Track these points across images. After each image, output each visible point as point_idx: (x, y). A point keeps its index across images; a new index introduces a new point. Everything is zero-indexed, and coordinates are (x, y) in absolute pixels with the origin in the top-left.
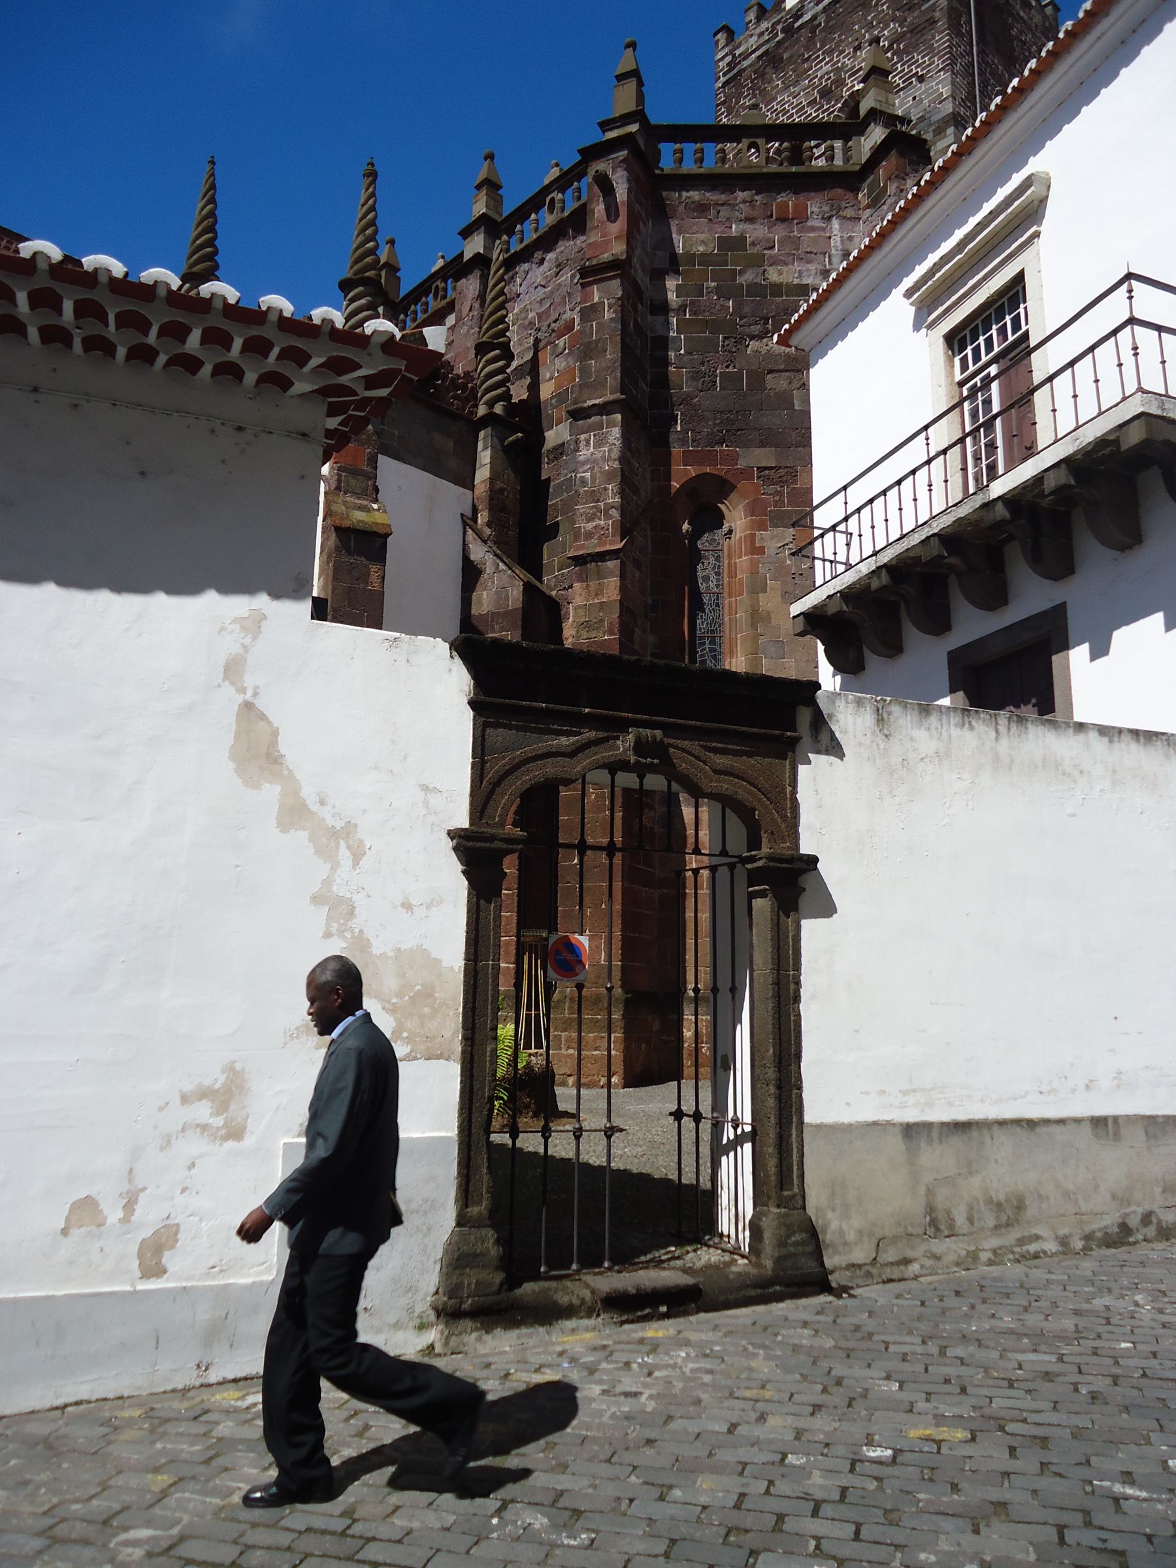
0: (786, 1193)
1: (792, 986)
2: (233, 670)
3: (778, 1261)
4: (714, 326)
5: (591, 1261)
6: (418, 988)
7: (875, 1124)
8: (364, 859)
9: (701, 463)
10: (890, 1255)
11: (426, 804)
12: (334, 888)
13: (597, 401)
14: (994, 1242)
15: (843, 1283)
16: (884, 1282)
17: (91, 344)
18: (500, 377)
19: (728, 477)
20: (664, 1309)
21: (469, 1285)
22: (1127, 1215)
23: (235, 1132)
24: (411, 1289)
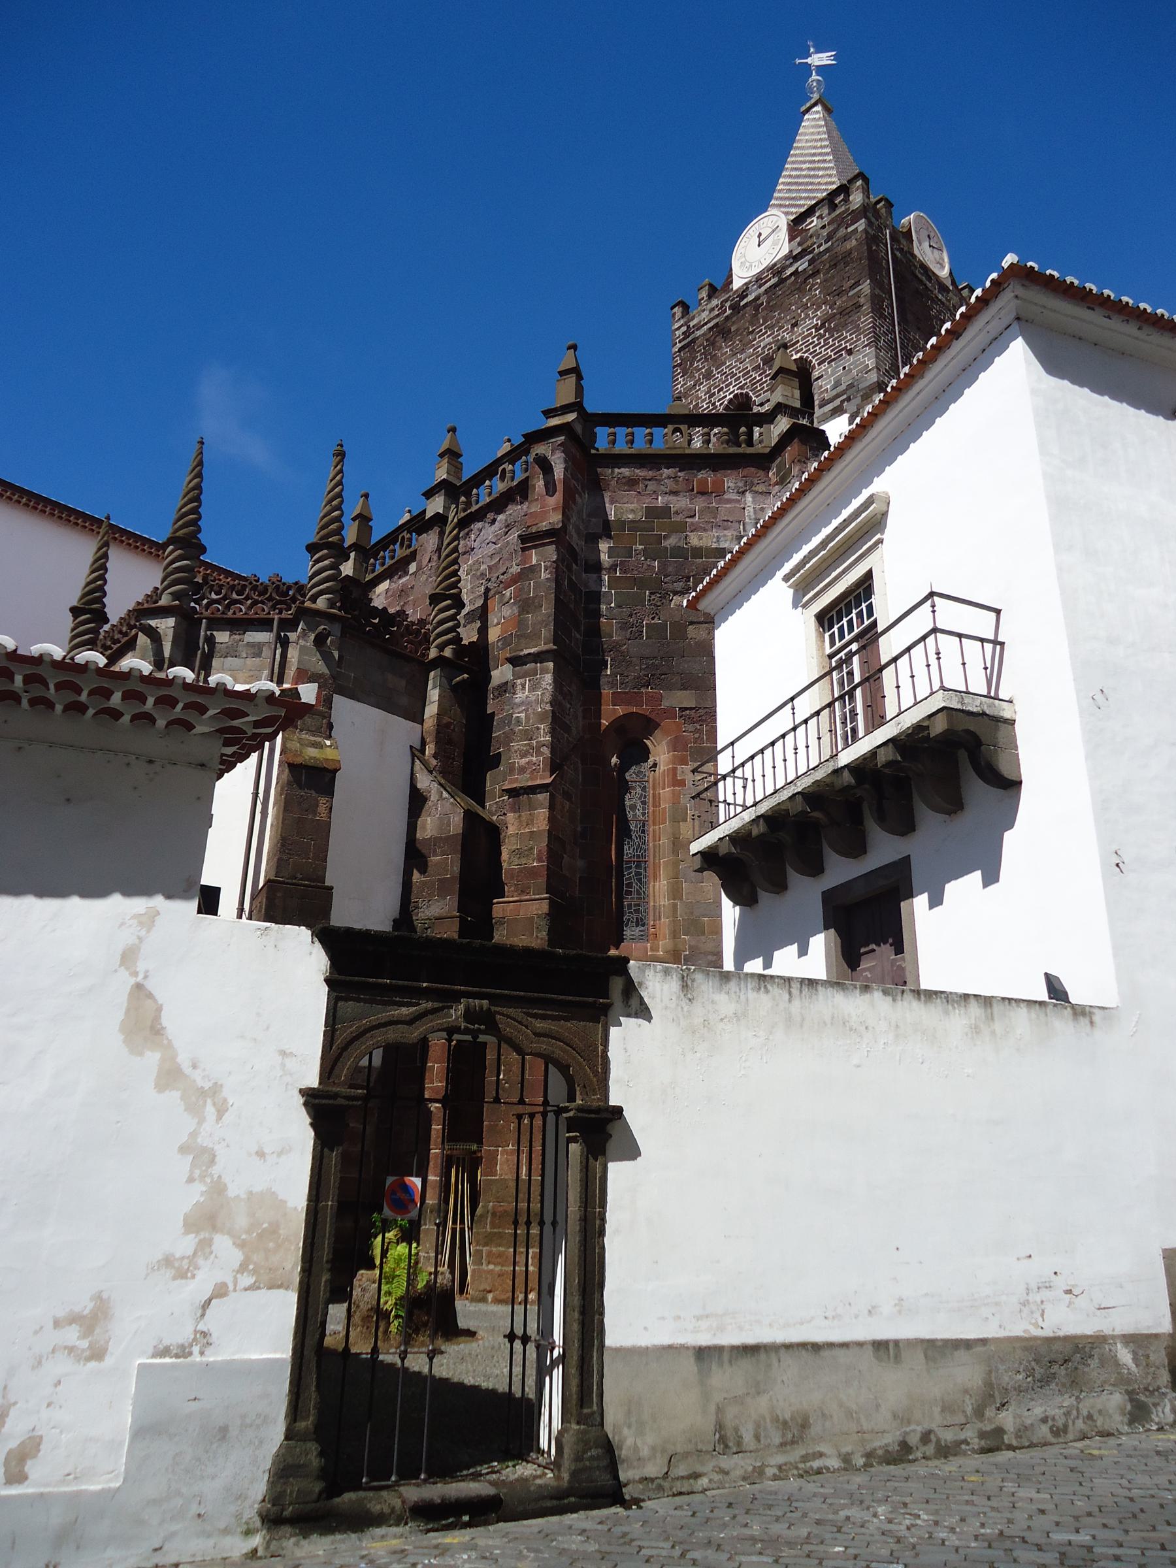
0: (585, 1411)
1: (598, 1222)
3: (574, 1474)
4: (640, 583)
5: (409, 1474)
6: (265, 1225)
7: (670, 1347)
8: (227, 1114)
9: (628, 703)
10: (681, 1470)
11: (283, 1065)
12: (199, 1140)
13: (532, 651)
14: (780, 1459)
15: (636, 1496)
16: (674, 1495)
17: (33, 702)
18: (451, 624)
19: (652, 716)
20: (466, 1518)
21: (291, 1492)
22: (906, 1433)
23: (98, 1354)
24: (241, 1497)
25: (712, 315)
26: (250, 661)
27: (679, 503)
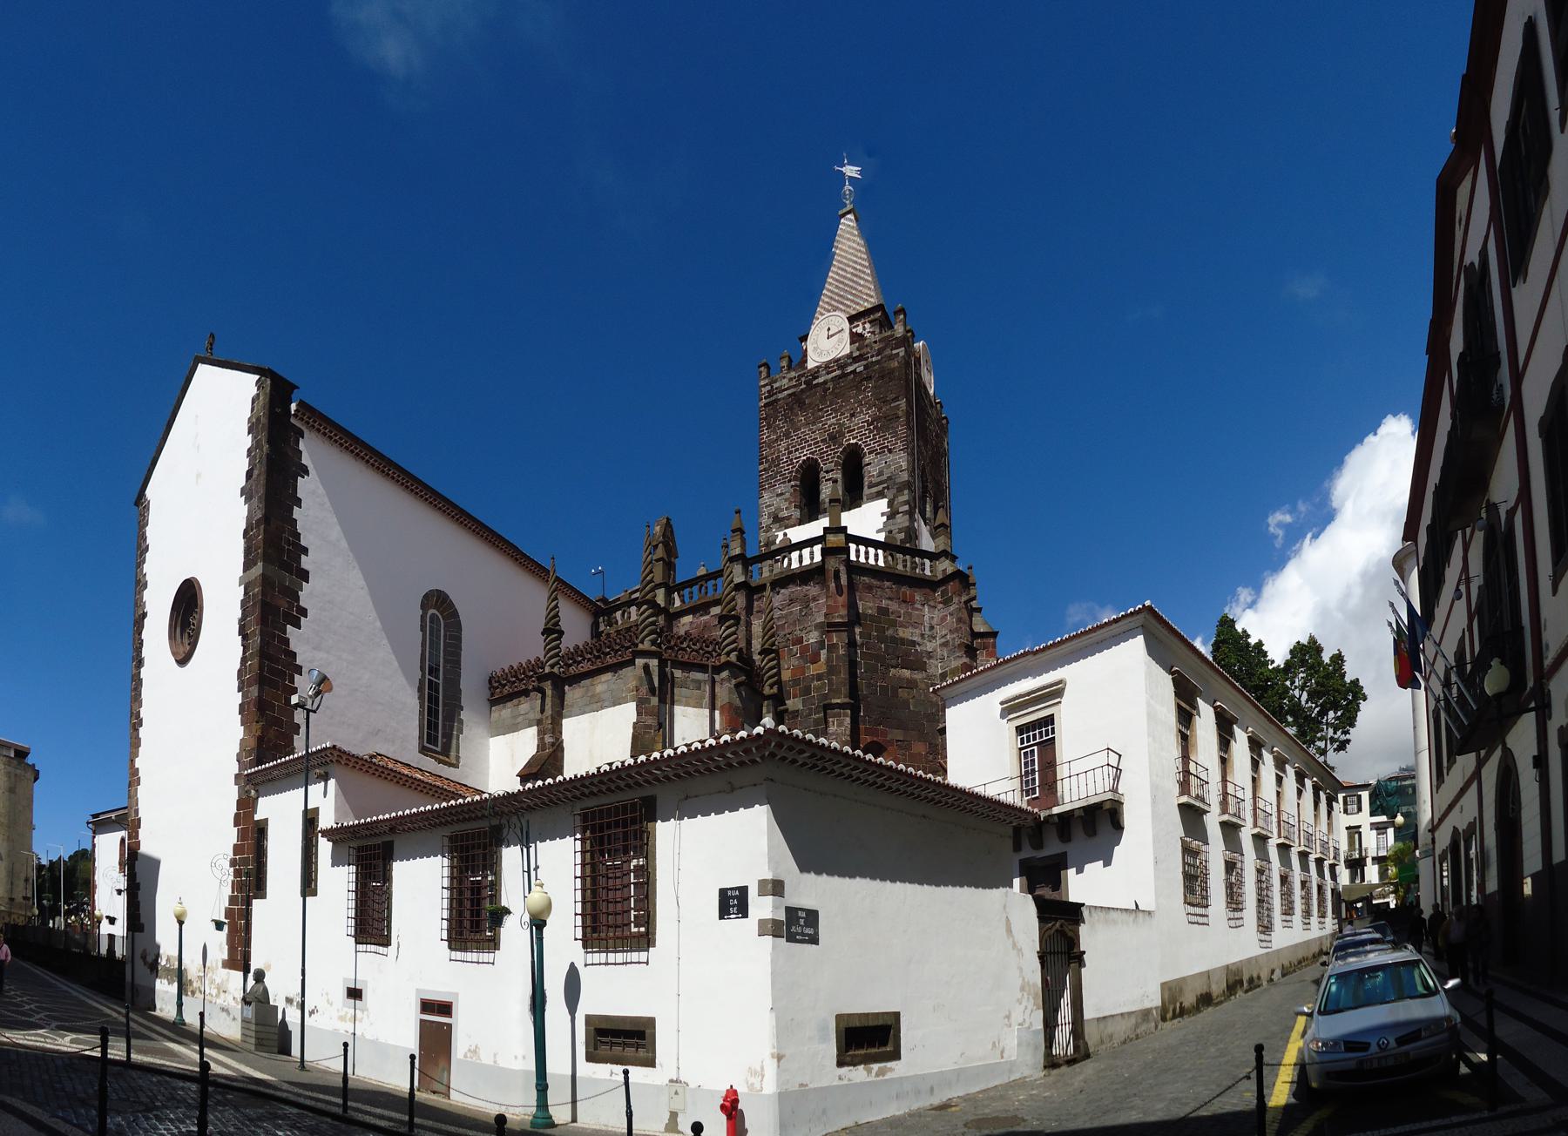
27: (893, 606)
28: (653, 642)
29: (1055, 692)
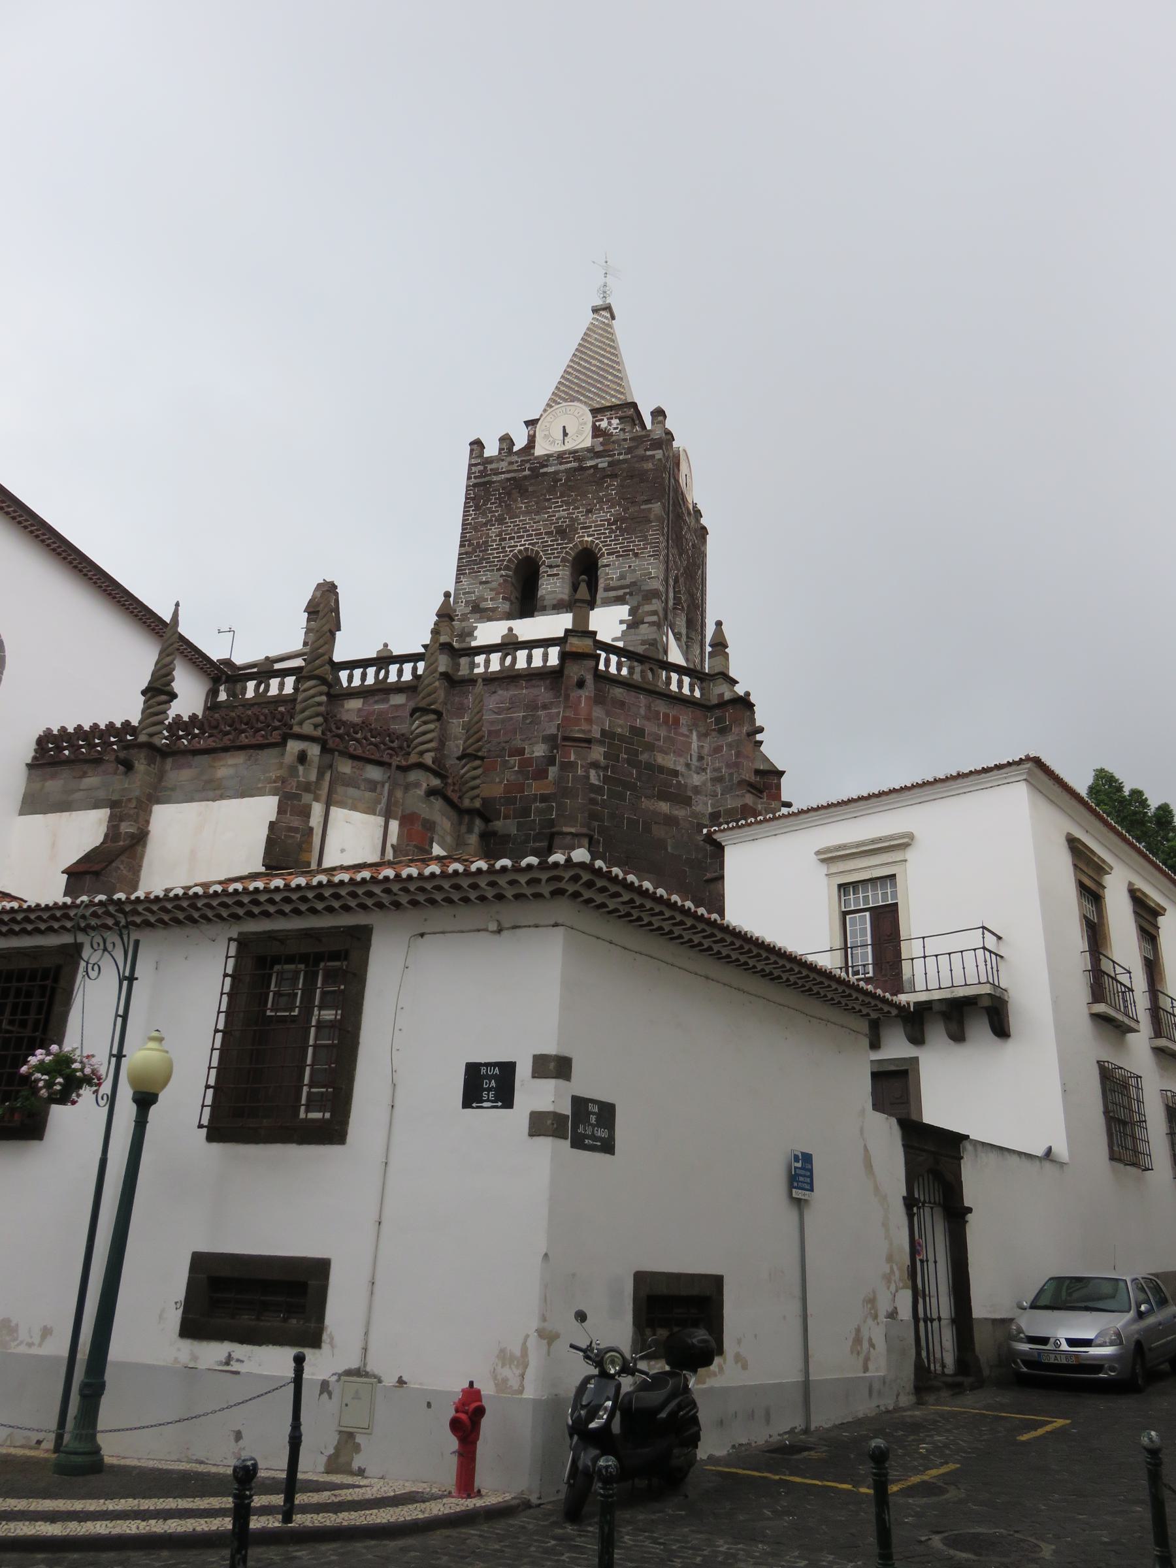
2: (862, 1130)
13: (573, 830)
25: (511, 468)
26: (368, 794)
27: (650, 728)
28: (316, 726)
29: (901, 844)
